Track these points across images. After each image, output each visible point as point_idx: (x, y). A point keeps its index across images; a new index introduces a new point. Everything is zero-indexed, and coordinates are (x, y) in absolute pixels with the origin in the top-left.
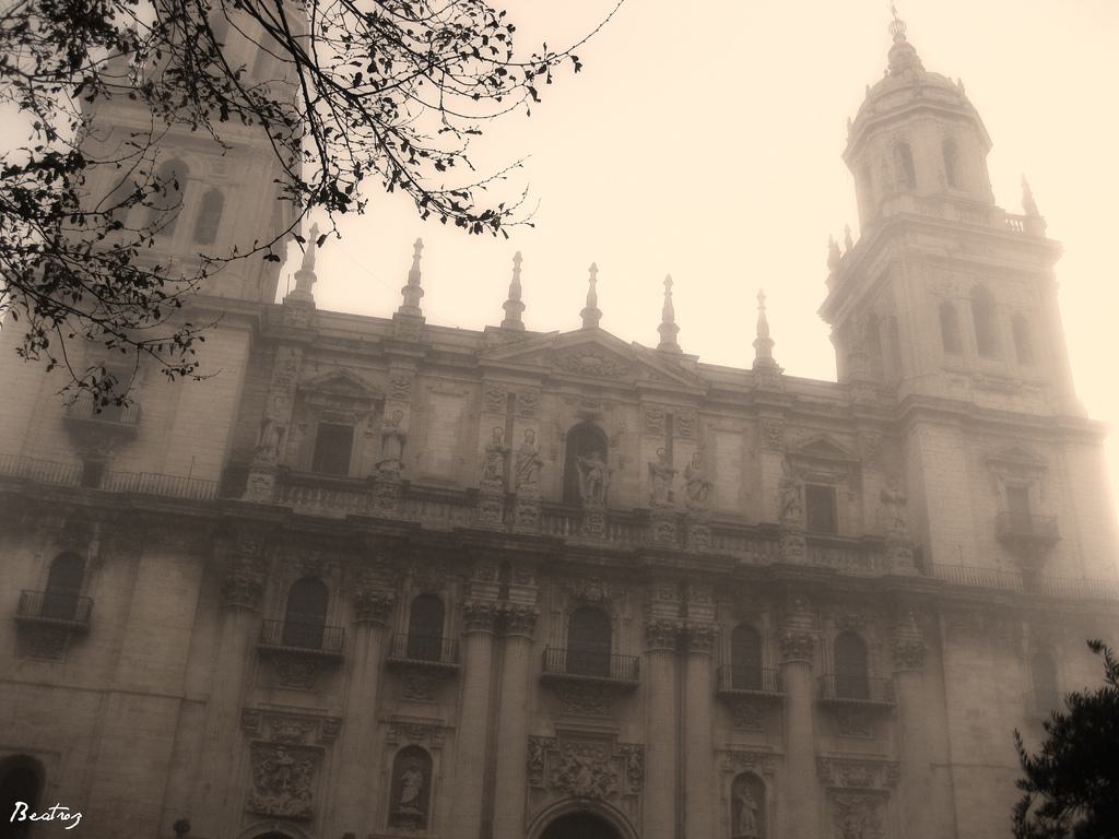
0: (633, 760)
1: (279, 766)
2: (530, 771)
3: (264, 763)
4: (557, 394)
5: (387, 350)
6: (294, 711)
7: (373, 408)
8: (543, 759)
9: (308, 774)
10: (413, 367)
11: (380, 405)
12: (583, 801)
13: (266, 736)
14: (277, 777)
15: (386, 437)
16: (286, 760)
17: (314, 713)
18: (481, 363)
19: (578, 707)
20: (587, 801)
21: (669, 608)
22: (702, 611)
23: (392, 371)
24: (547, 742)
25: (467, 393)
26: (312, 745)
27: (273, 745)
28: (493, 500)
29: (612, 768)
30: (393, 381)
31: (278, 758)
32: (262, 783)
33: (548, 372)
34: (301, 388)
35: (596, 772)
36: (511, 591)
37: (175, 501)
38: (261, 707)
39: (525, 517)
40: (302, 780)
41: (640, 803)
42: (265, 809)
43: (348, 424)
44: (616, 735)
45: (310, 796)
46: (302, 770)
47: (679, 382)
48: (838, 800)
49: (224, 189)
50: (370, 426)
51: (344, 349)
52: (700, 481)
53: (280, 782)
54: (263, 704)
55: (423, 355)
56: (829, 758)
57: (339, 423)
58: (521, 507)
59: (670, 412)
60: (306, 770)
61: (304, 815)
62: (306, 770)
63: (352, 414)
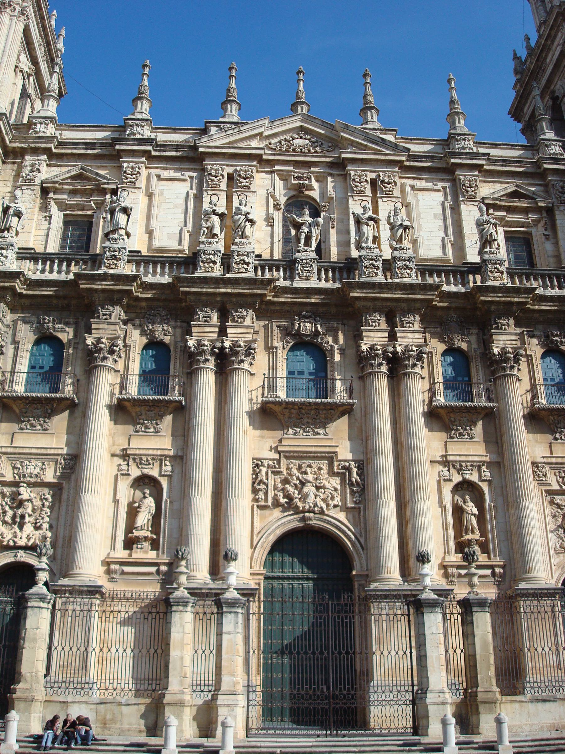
0: (355, 475)
2: (255, 491)
4: (272, 172)
6: (34, 451)
7: (108, 196)
8: (267, 479)
12: (307, 514)
17: (52, 451)
18: (201, 150)
19: (298, 430)
20: (312, 515)
21: (379, 334)
22: (410, 335)
23: (125, 165)
24: (271, 463)
25: (191, 177)
27: (16, 484)
28: (210, 254)
29: (336, 482)
31: (20, 494)
34: (44, 185)
35: (318, 488)
36: (229, 330)
39: (240, 266)
41: (362, 513)
44: (335, 453)
48: (558, 501)
52: (401, 224)
53: (23, 517)
56: (544, 463)
58: (236, 257)
59: (374, 177)
62: (47, 504)
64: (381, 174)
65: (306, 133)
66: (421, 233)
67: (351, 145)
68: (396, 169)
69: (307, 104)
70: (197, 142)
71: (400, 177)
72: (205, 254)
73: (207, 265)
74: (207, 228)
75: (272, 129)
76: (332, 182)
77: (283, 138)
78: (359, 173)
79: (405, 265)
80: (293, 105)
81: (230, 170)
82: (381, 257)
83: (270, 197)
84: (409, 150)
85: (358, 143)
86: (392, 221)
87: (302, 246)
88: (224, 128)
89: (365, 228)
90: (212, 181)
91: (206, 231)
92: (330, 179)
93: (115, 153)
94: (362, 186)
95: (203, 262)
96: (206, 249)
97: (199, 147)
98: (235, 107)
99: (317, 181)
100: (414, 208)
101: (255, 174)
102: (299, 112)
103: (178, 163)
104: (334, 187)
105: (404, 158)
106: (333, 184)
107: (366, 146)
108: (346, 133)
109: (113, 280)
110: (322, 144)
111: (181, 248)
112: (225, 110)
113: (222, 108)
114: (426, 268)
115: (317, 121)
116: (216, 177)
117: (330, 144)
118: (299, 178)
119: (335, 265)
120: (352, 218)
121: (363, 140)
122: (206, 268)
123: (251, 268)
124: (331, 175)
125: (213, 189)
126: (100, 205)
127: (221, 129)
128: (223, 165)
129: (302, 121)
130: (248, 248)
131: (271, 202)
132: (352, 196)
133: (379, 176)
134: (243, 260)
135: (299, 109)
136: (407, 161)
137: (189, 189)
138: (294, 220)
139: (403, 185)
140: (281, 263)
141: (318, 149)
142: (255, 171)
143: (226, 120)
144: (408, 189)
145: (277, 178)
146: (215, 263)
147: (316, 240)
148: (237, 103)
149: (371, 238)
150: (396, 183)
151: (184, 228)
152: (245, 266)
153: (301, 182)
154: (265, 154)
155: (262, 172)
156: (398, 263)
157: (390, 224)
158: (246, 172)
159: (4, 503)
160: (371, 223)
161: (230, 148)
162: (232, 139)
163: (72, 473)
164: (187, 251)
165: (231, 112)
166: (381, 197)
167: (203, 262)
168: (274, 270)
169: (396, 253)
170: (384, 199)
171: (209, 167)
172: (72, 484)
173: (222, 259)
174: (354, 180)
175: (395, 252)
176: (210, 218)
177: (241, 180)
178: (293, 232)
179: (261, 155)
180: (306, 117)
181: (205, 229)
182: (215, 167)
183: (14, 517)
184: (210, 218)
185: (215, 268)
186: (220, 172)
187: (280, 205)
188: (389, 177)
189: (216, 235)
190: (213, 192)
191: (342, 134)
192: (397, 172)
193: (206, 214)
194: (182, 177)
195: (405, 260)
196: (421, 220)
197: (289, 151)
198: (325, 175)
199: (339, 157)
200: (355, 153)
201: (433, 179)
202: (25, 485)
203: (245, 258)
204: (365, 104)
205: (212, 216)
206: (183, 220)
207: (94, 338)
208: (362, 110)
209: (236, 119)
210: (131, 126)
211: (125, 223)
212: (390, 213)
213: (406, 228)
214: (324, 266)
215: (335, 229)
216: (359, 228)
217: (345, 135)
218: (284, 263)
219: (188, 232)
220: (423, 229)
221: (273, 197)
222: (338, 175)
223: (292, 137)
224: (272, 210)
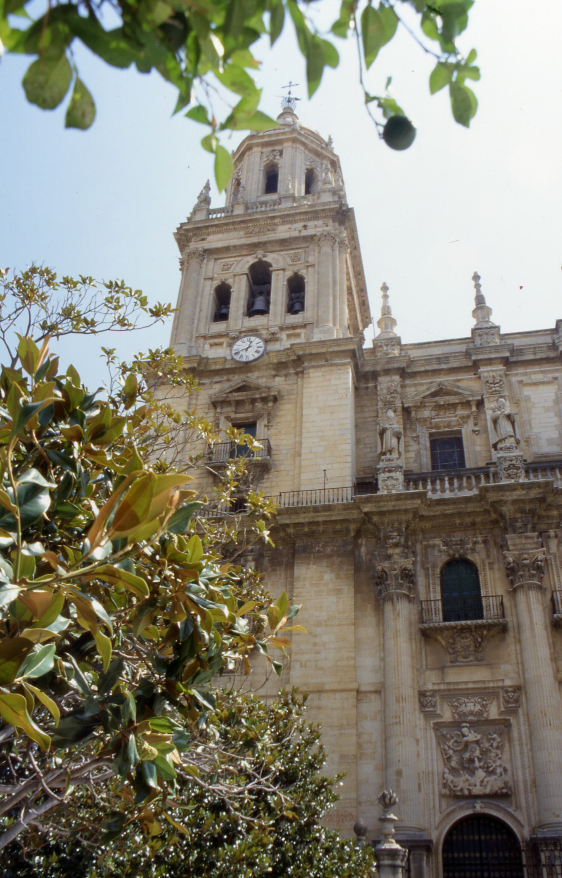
1: (467, 744)
3: (450, 743)
5: (474, 358)
6: (470, 686)
7: (474, 408)
9: (497, 748)
10: (501, 367)
11: (480, 404)
13: (447, 715)
14: (467, 755)
15: (495, 421)
16: (471, 736)
17: (491, 685)
25: (556, 379)
26: (497, 717)
27: (456, 725)
30: (487, 382)
31: (464, 736)
32: (453, 764)
34: (405, 405)
37: (316, 510)
38: (436, 687)
40: (493, 755)
42: (462, 790)
43: (455, 429)
45: (505, 770)
46: (492, 746)
49: (303, 272)
50: (476, 424)
51: (436, 367)
53: (471, 761)
54: (438, 684)
55: (507, 354)
57: (447, 429)
60: (495, 744)
61: (505, 791)
62: (495, 744)
63: (457, 418)
93: (470, 364)
109: (523, 489)
126: (465, 419)
159: (446, 748)
163: (519, 707)
172: (521, 719)
183: (461, 762)
202: (468, 725)
207: (514, 555)
210: (480, 335)
211: (511, 430)
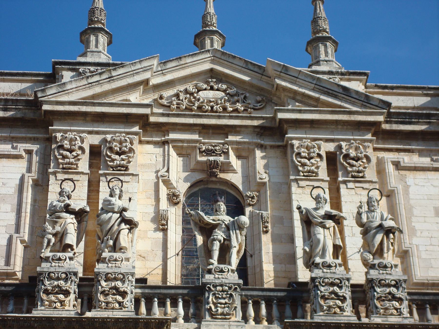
4: (165, 143)
18: (45, 107)
25: (29, 152)
28: (58, 279)
33: (147, 111)
39: (110, 298)
47: (340, 107)
52: (381, 226)
58: (103, 283)
64: (343, 144)
65: (219, 81)
66: (415, 241)
67: (294, 99)
68: (369, 136)
69: (221, 35)
70: (39, 95)
71: (375, 149)
72: (50, 278)
73: (53, 298)
74: (55, 235)
75: (163, 74)
76: (263, 158)
77: (182, 88)
78: (308, 143)
79: (390, 293)
80: (197, 36)
81: (96, 140)
82: (348, 280)
83: (161, 184)
84: (388, 105)
85: (304, 95)
86: (364, 218)
87: (216, 263)
88: (84, 72)
89: (320, 233)
90: (64, 157)
91: (53, 240)
92: (259, 154)
94: (313, 165)
95: (46, 292)
96: (52, 270)
97: (42, 103)
98: (103, 39)
99: (239, 157)
100: (400, 198)
101: (137, 147)
102: (208, 45)
103: (8, 130)
104: (266, 167)
105: (381, 118)
106: (264, 162)
107: (317, 100)
108: (285, 80)
110: (245, 98)
111: (9, 269)
112: (87, 43)
113: (82, 41)
114: (426, 298)
115: (236, 61)
116: (71, 151)
117: (259, 98)
118: (209, 152)
119: (272, 294)
120: (296, 216)
121: (313, 90)
122: (51, 302)
123: (129, 302)
124: (262, 147)
125: (65, 170)
127: (80, 74)
128: (83, 132)
129: (212, 62)
130: (125, 267)
131: (164, 191)
132: (296, 180)
133: (340, 147)
134: (116, 288)
135: (208, 42)
136: (386, 122)
137: (24, 171)
138: (201, 219)
139: (380, 163)
140: (180, 291)
141: (239, 106)
142: (136, 142)
143: (89, 59)
144: (390, 168)
145: (173, 153)
146: (67, 293)
147: (238, 252)
148: (107, 33)
149: (330, 250)
150: (368, 158)
151: (15, 236)
152: (119, 298)
153: (212, 158)
154: (153, 114)
155: (148, 142)
156: (378, 290)
157: (360, 224)
158: (121, 143)
160: (330, 223)
161: (94, 104)
162: (98, 90)
164: (19, 275)
165: (97, 46)
166: (345, 182)
167: (46, 292)
168: (168, 303)
169: (374, 274)
170: (351, 185)
171: (59, 135)
173: (79, 286)
174: (299, 154)
175: (372, 272)
176: (59, 218)
177: (114, 156)
178: (200, 240)
179: (146, 116)
180: (218, 55)
181: (50, 236)
182: (70, 135)
184: (59, 218)
185: (67, 302)
186: (78, 143)
187: (177, 196)
188: (357, 149)
189: (71, 246)
190: (66, 176)
191: (278, 81)
192: (370, 141)
193: (54, 211)
194: (14, 152)
195: (389, 286)
196: (414, 219)
197: (191, 110)
198: (251, 147)
199: (274, 118)
200: (300, 111)
201: (431, 151)
203: (119, 284)
204: (314, 33)
205: (64, 215)
206: (13, 222)
208: (309, 43)
209: (104, 58)
212: (361, 207)
213: (388, 231)
214: (252, 297)
215: (269, 235)
216: (309, 232)
217: (284, 84)
218: (185, 291)
219: (22, 242)
220: (418, 234)
221: (167, 183)
222: (272, 147)
223: (196, 86)
224: (164, 204)
